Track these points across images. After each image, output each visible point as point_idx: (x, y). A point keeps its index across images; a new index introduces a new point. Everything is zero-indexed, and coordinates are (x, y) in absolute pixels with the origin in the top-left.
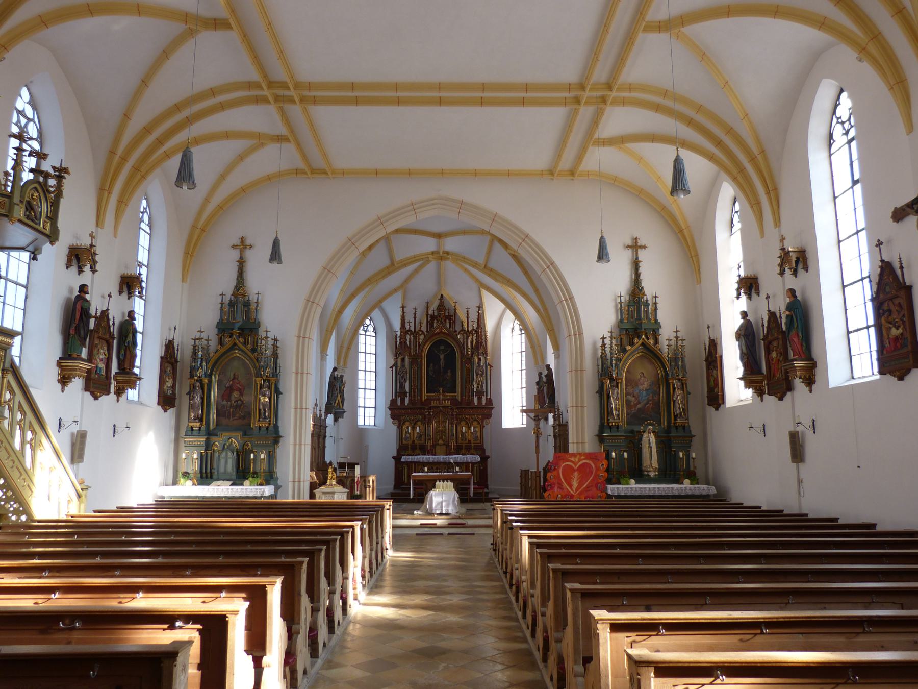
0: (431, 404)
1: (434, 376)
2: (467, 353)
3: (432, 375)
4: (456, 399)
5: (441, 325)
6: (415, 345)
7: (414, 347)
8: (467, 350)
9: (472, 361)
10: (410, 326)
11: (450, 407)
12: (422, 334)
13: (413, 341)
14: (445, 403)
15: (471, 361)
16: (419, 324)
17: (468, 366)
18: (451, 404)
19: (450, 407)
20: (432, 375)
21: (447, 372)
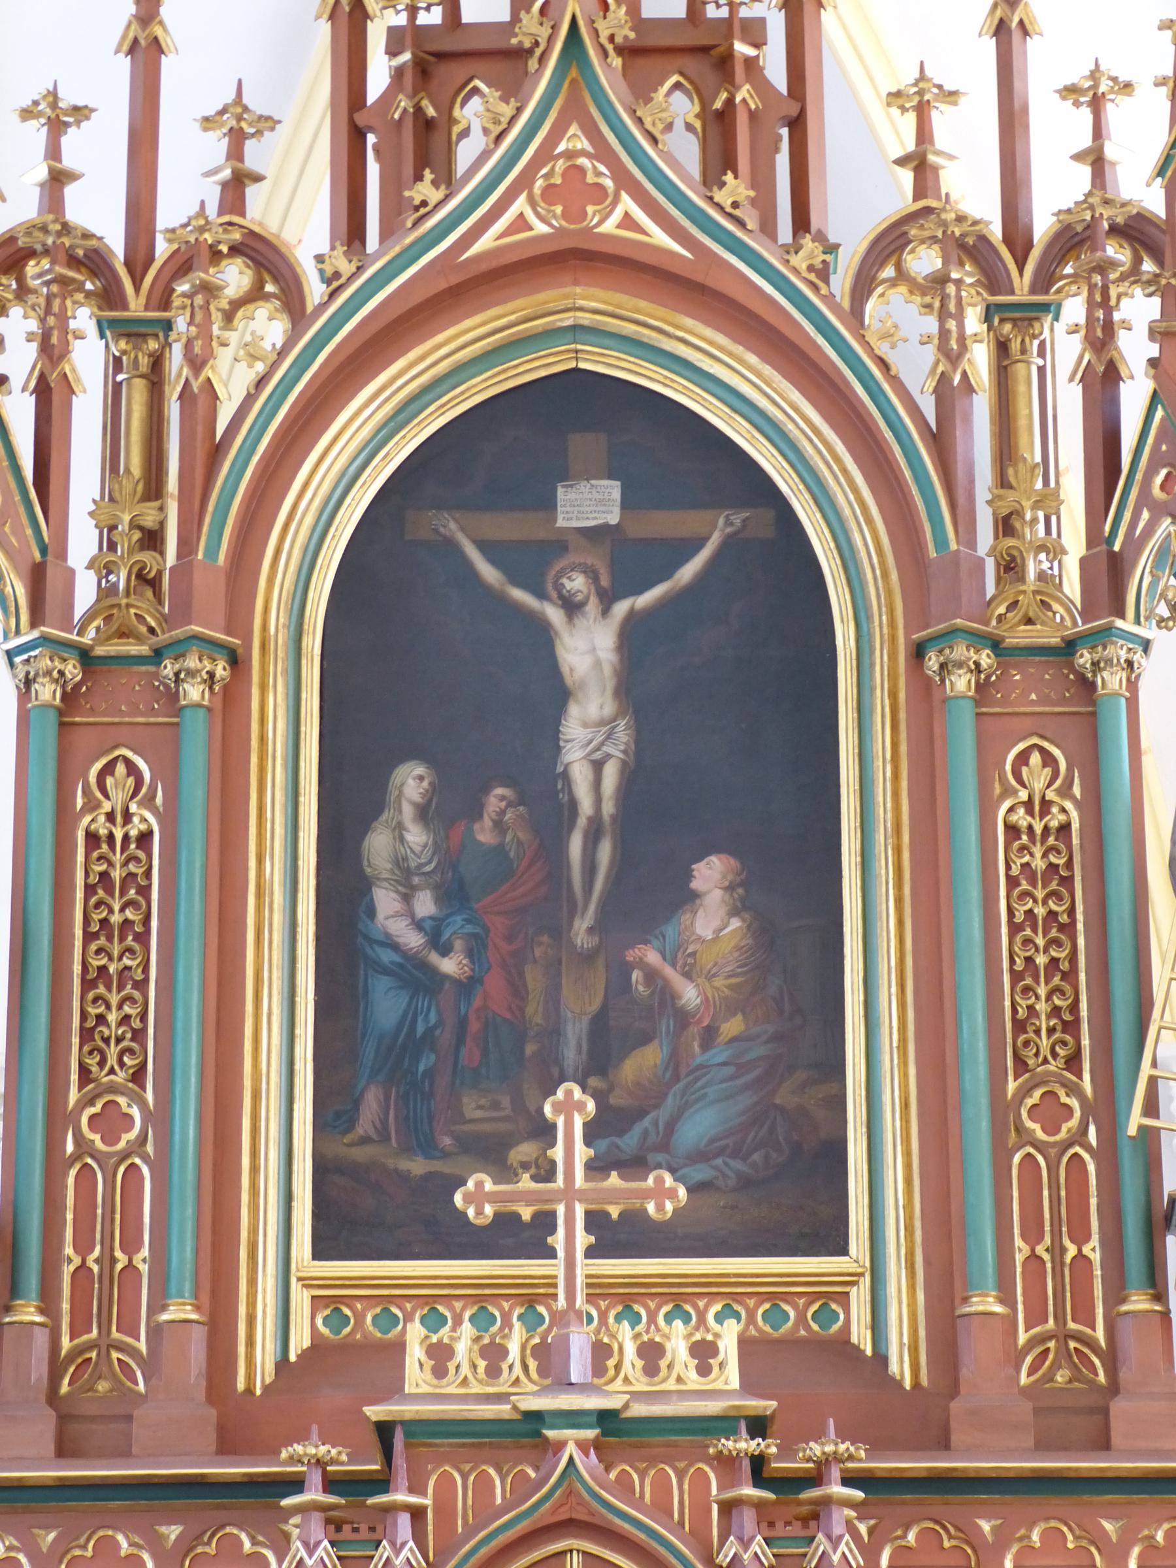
0: (394, 1388)
1: (449, 965)
2: (1010, 568)
3: (413, 940)
4: (843, 1345)
5: (575, 140)
6: (134, 460)
7: (110, 497)
8: (1006, 525)
9: (1112, 681)
10: (58, 179)
11: (758, 1426)
12: (255, 295)
13: (115, 396)
14: (651, 1353)
15: (1087, 686)
16: (216, 146)
17: (1037, 777)
18: (749, 1385)
19: (758, 1426)
20: (413, 940)
21: (694, 896)
